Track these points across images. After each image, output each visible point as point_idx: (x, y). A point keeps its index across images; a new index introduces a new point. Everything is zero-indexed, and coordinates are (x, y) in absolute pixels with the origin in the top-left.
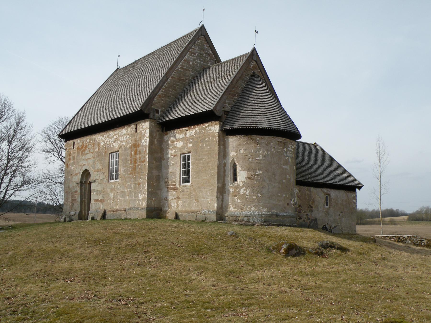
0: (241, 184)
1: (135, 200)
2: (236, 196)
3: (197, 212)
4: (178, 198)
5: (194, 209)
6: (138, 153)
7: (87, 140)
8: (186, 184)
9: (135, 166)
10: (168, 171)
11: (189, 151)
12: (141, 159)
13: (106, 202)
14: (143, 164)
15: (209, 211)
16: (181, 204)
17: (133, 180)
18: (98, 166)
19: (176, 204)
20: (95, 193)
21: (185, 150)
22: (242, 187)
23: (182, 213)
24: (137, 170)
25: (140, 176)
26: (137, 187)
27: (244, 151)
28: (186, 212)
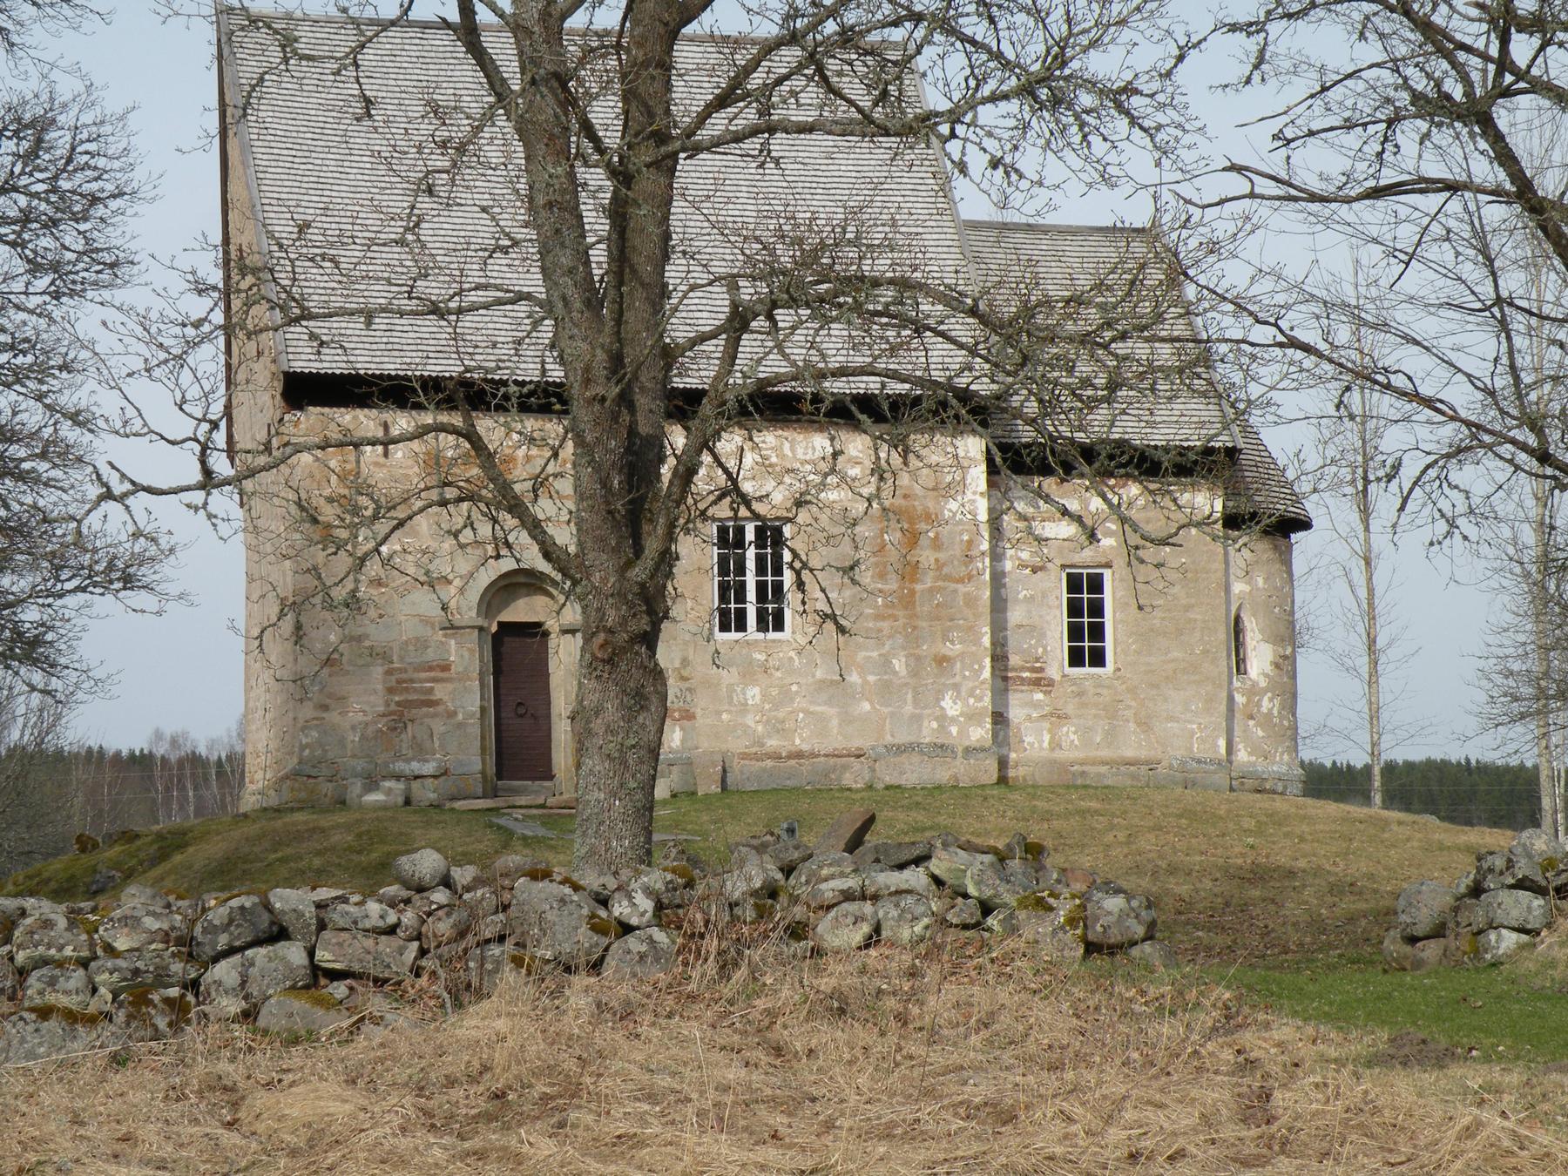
0: (1263, 683)
1: (916, 719)
2: (1251, 717)
3: (1147, 763)
4: (1059, 717)
5: (1130, 753)
6: (923, 541)
8: (1087, 670)
9: (912, 593)
10: (1006, 621)
11: (1104, 561)
12: (945, 570)
14: (962, 588)
15: (1199, 761)
16: (1072, 736)
17: (900, 640)
19: (1047, 737)
21: (1088, 555)
23: (1084, 768)
24: (923, 608)
25: (949, 629)
26: (930, 668)
27: (1266, 580)
28: (1104, 763)
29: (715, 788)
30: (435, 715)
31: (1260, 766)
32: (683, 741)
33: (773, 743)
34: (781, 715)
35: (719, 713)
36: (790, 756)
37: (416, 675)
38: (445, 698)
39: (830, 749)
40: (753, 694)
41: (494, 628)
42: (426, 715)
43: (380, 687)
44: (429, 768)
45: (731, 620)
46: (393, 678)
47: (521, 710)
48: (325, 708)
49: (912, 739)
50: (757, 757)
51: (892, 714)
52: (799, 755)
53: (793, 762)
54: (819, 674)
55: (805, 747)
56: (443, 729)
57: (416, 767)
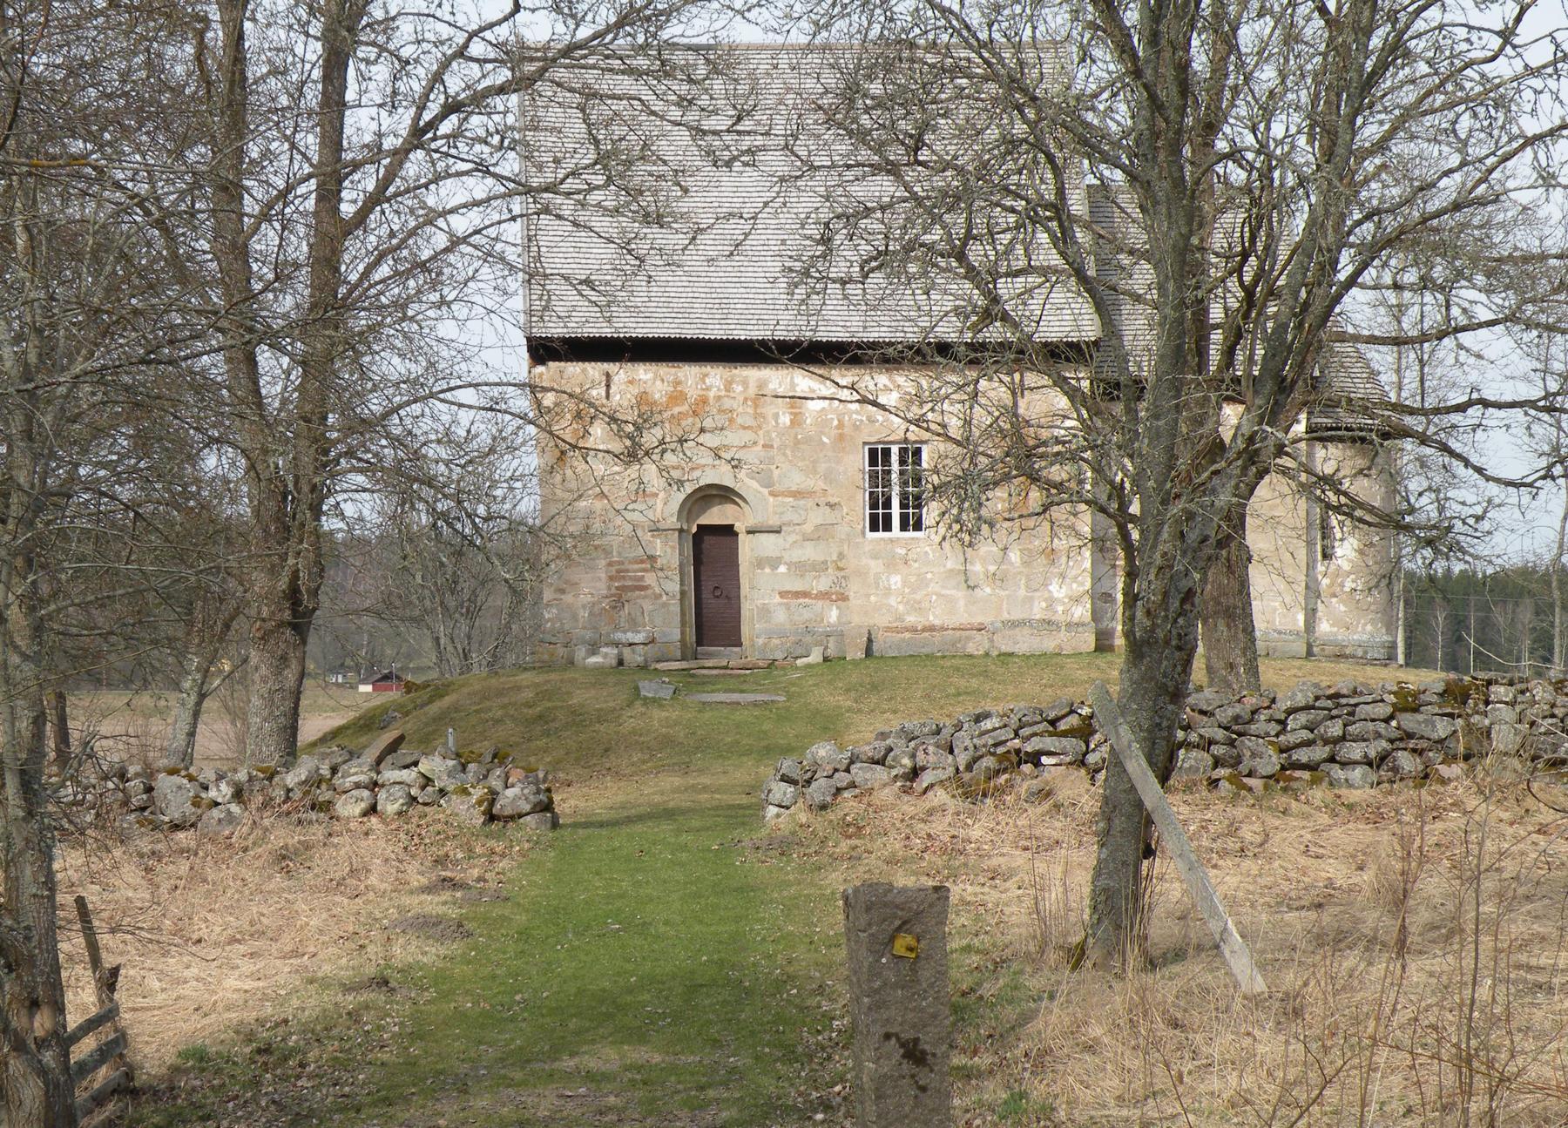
0: (1346, 566)
7: (714, 376)
13: (854, 602)
15: (1280, 633)
18: (796, 480)
20: (782, 569)
22: (1349, 574)
29: (861, 655)
30: (645, 597)
31: (1342, 635)
32: (839, 617)
33: (911, 619)
34: (918, 597)
35: (868, 596)
36: (924, 630)
39: (957, 625)
40: (896, 581)
41: (694, 530)
43: (603, 575)
44: (639, 638)
45: (879, 522)
46: (614, 569)
48: (562, 591)
49: (1025, 616)
50: (898, 630)
51: (1009, 596)
52: (932, 629)
53: (926, 634)
54: (949, 565)
55: (937, 622)
57: (631, 637)
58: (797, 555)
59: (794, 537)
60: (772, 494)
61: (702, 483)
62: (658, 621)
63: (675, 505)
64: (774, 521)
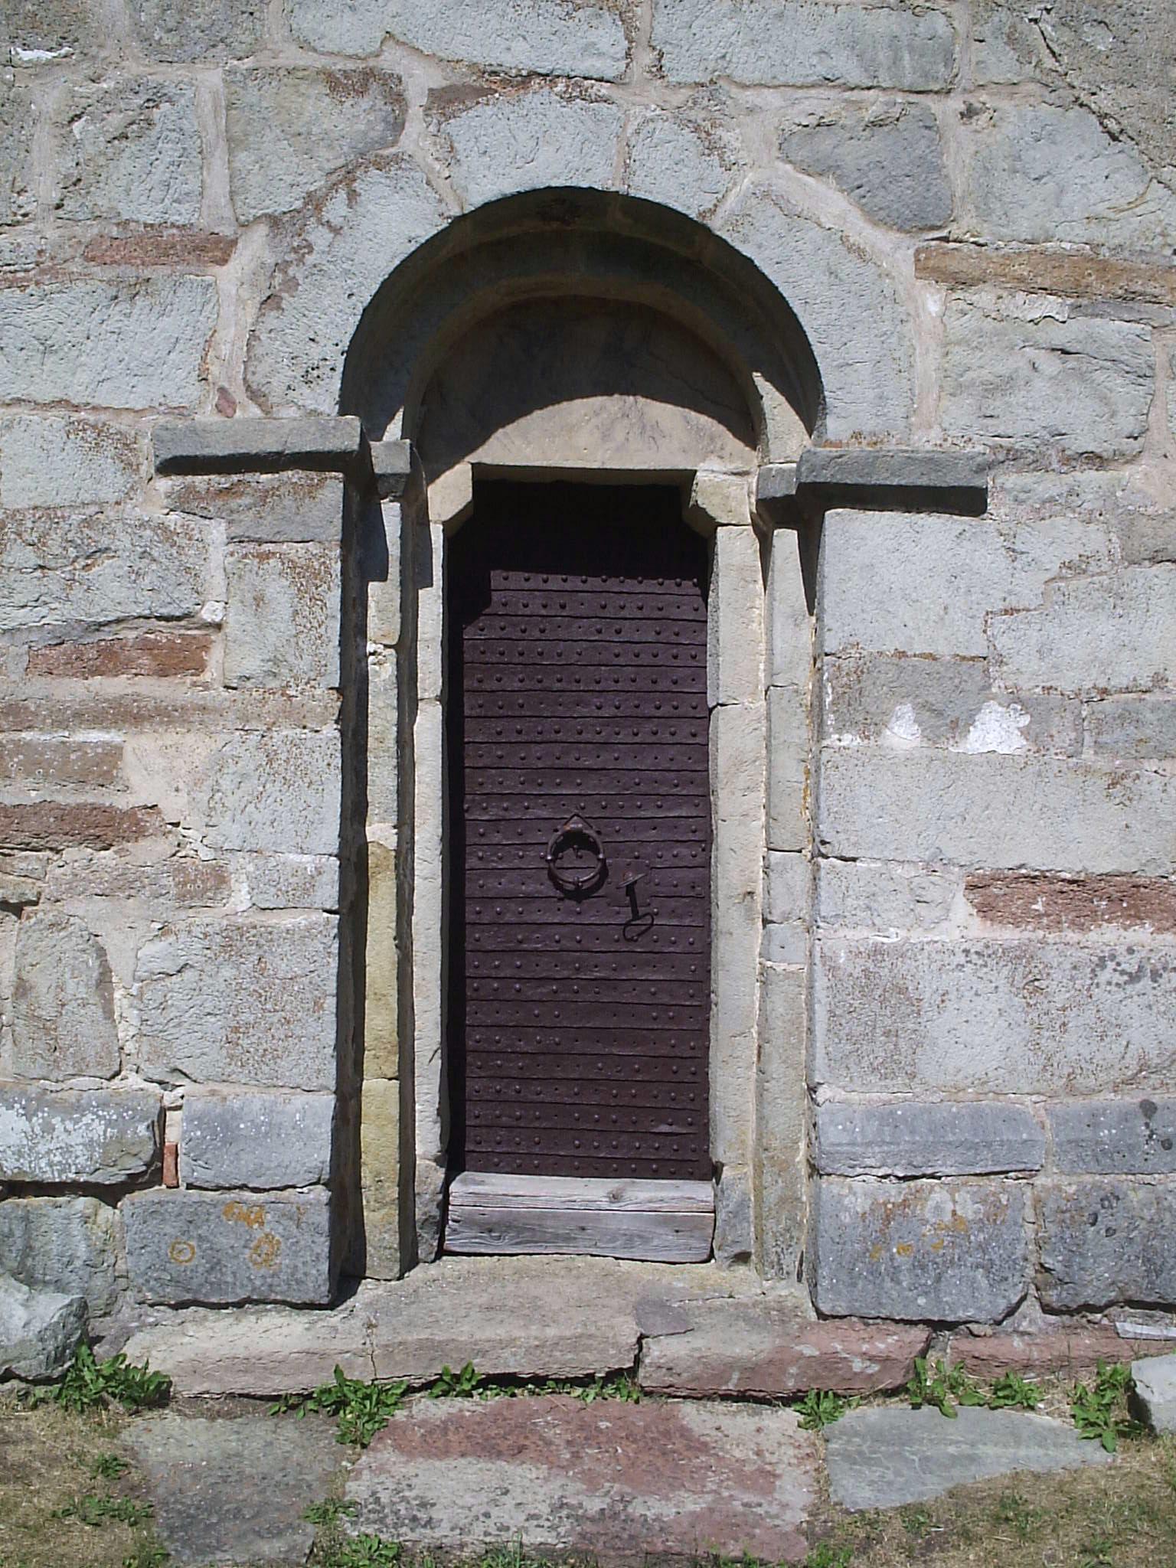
20: (996, 732)
30: (123, 886)
37: (37, 688)
38: (173, 806)
42: (73, 888)
47: (579, 871)
56: (156, 953)
58: (1083, 646)
59: (1060, 540)
60: (927, 268)
61: (487, 183)
62: (197, 1047)
63: (330, 318)
64: (938, 432)
